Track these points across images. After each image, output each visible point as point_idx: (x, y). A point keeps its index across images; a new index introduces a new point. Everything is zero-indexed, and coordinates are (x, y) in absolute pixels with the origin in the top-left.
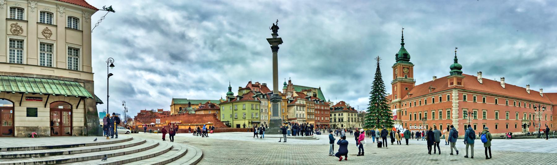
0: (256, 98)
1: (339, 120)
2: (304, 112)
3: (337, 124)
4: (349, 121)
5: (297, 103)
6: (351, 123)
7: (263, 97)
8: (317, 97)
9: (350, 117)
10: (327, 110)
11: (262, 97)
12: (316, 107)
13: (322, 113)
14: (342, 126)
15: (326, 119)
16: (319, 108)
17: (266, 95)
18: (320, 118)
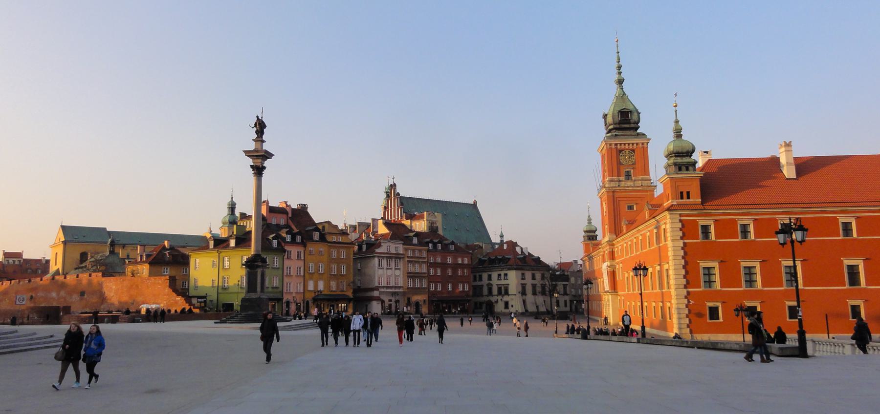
0: (275, 243)
1: (500, 289)
2: (398, 272)
3: (493, 299)
4: (523, 293)
5: (377, 250)
6: (530, 297)
8: (440, 232)
9: (529, 281)
10: (463, 266)
11: (289, 238)
12: (432, 260)
13: (449, 272)
14: (507, 304)
15: (460, 288)
16: (439, 260)
17: (298, 234)
18: (444, 287)
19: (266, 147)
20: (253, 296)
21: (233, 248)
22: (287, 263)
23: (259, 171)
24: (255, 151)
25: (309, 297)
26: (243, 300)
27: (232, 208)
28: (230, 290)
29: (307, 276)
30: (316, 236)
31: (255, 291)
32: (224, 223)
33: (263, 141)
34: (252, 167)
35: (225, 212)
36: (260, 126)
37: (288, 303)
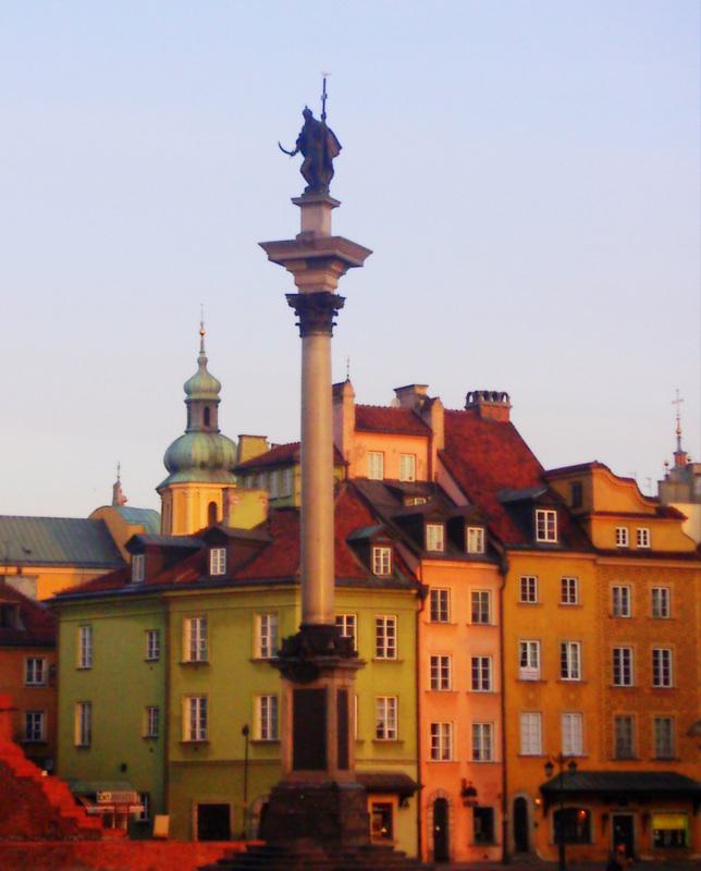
0: (382, 556)
7: (455, 540)
11: (435, 535)
19: (339, 225)
20: (310, 778)
21: (220, 582)
22: (435, 642)
23: (316, 312)
24: (307, 239)
25: (528, 783)
26: (280, 794)
27: (203, 408)
29: (513, 692)
30: (548, 522)
31: (320, 762)
32: (174, 465)
33: (334, 204)
34: (293, 300)
36: (317, 147)
37: (441, 807)
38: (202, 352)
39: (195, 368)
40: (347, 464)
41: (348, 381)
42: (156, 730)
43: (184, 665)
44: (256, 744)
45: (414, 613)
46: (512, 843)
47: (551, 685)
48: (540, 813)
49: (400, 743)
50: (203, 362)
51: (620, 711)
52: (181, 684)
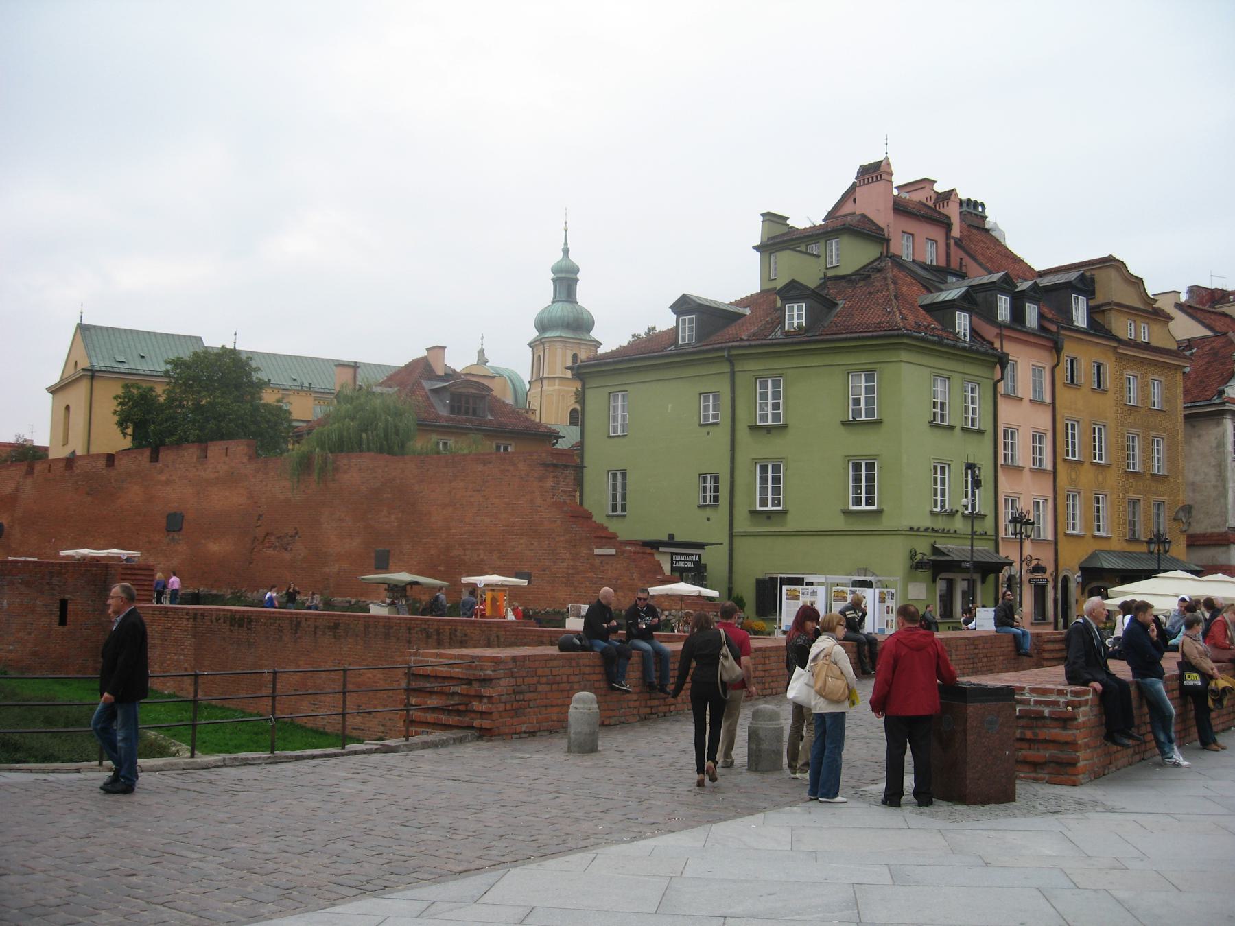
7: (1018, 314)
28: (792, 524)
35: (543, 295)
38: (566, 243)
39: (561, 255)
40: (888, 241)
41: (887, 158)
42: (716, 499)
43: (754, 428)
44: (847, 512)
45: (992, 382)
46: (1061, 621)
47: (1087, 465)
48: (1080, 590)
49: (983, 517)
50: (566, 251)
51: (1131, 495)
52: (750, 448)
